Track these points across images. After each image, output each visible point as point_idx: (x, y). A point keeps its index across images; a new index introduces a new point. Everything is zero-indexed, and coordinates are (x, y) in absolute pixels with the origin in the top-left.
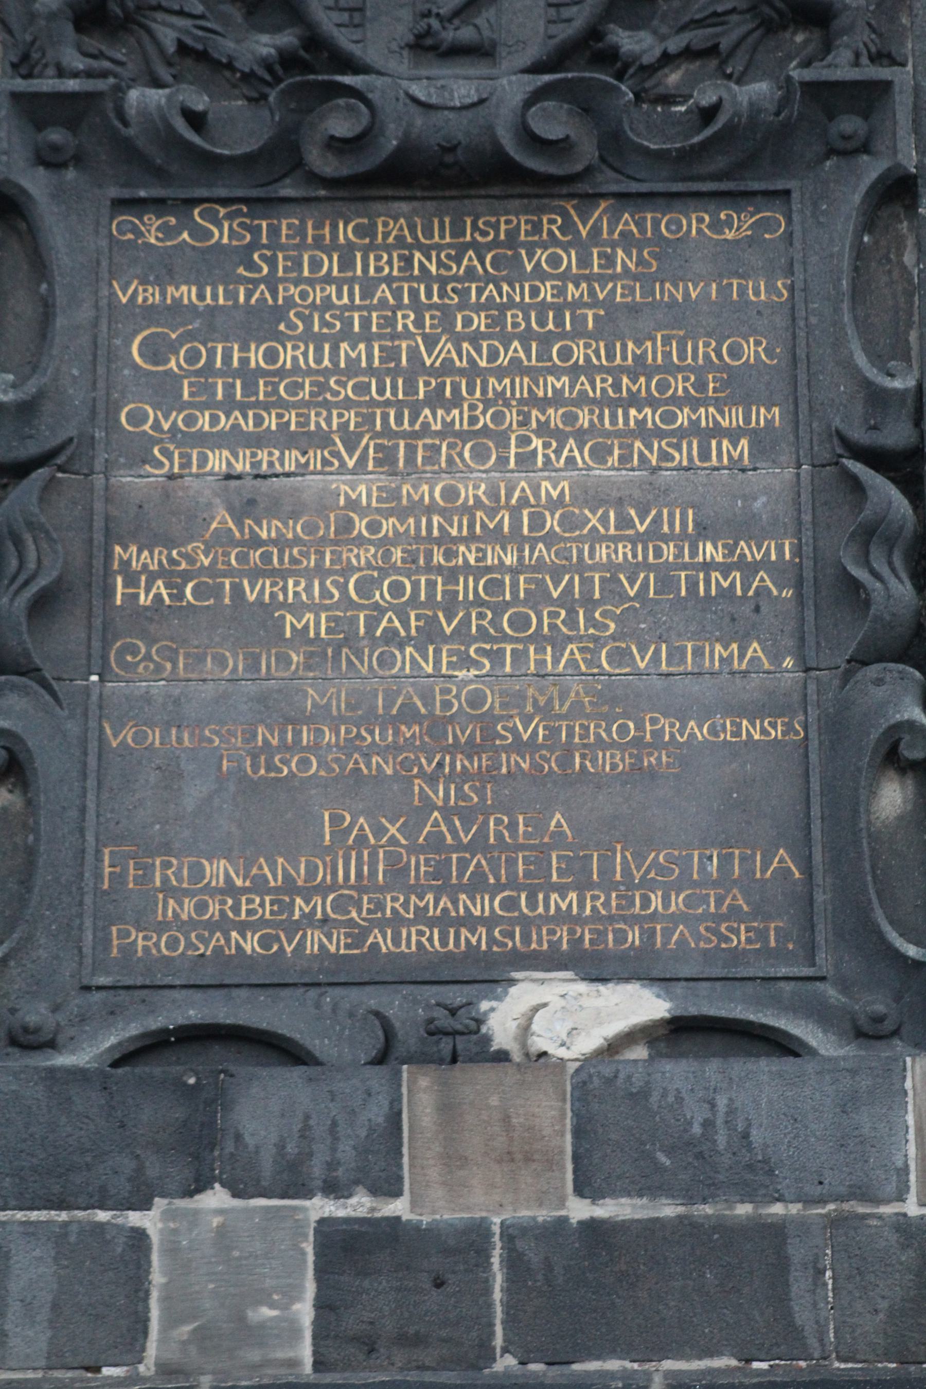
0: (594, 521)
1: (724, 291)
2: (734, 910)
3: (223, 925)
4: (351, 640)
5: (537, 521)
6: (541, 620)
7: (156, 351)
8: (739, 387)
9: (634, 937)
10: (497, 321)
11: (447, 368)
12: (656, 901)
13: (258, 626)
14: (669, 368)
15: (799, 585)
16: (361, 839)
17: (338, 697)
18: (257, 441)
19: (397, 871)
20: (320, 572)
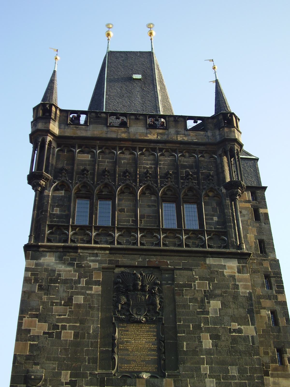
0: (146, 344)
1: (153, 330)
2: (154, 369)
3: (126, 369)
4: (133, 351)
5: (143, 344)
6: (143, 350)
7: (122, 332)
8: (154, 336)
9: (149, 370)
10: (141, 331)
11: (138, 334)
12: (150, 368)
13: (127, 350)
14: (150, 334)
15: (158, 349)
16: (133, 364)
17: (132, 355)
18: (127, 338)
19: (135, 366)
20: (131, 347)
